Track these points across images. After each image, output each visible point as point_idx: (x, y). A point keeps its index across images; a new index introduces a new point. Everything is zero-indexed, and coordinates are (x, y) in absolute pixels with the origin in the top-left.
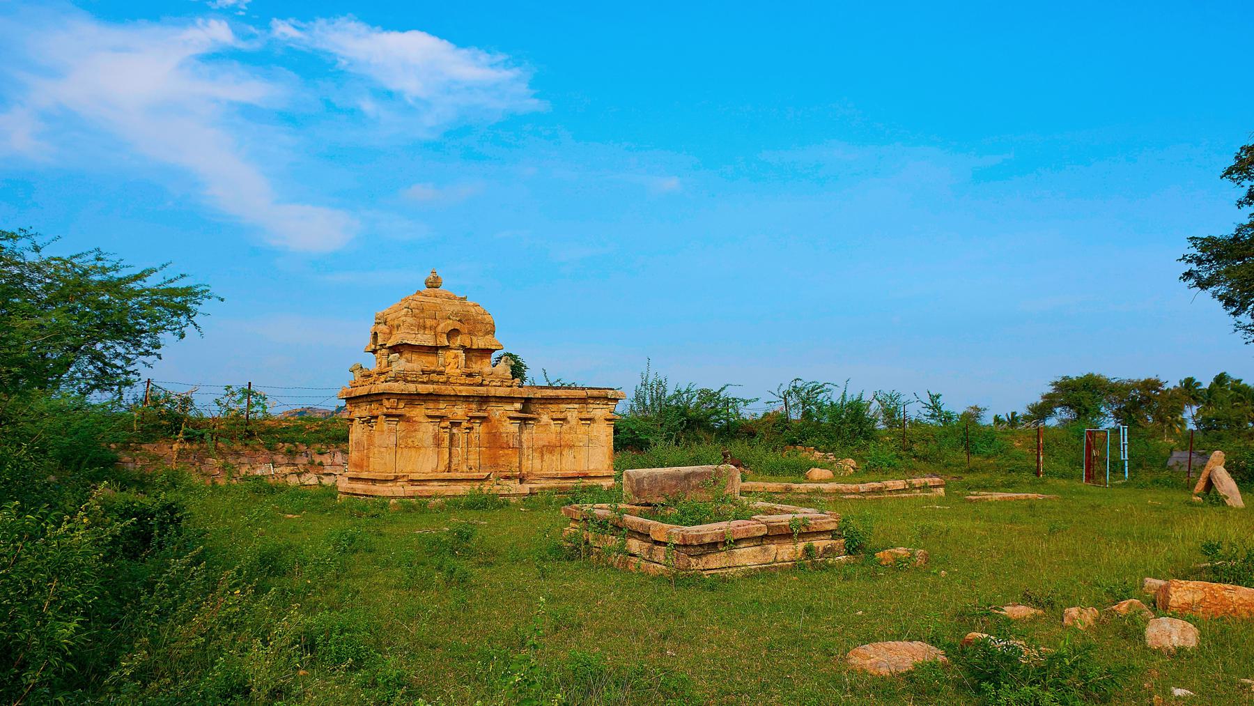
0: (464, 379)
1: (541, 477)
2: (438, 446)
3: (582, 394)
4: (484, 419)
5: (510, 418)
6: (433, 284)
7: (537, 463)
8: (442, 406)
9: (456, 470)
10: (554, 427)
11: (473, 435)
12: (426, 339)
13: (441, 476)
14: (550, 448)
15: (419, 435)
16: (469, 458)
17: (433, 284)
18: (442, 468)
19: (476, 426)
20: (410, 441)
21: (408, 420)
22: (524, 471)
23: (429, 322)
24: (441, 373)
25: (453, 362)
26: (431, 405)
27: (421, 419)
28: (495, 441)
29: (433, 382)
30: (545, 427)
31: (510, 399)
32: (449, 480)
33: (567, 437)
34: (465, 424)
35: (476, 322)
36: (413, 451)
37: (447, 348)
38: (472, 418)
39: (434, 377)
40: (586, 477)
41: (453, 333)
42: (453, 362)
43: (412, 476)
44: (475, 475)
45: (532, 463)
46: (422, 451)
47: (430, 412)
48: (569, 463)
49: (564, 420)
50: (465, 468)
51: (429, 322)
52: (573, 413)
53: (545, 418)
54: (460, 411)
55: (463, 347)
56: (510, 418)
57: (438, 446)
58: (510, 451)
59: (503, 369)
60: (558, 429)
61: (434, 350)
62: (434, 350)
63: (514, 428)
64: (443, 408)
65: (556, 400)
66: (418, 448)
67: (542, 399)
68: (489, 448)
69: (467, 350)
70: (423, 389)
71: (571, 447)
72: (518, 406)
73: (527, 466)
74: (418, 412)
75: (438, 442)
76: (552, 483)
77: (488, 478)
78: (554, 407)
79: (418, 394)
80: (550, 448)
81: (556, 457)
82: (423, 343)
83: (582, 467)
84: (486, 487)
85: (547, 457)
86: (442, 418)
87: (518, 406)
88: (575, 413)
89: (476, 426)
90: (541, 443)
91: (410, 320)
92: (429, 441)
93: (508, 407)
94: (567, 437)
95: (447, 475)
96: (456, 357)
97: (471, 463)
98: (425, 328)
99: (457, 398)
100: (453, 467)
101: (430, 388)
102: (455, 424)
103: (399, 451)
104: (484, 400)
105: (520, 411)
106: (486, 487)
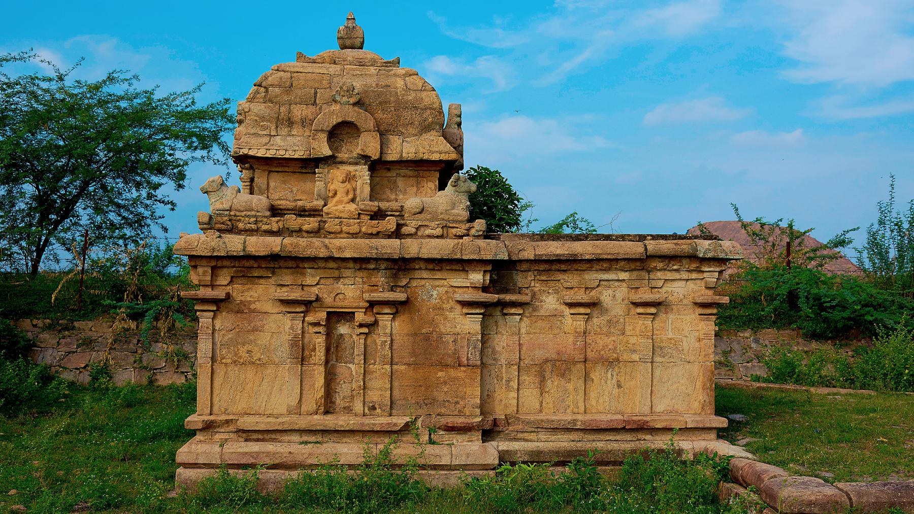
0: (368, 225)
1: (538, 427)
2: (303, 360)
3: (636, 249)
4: (399, 307)
5: (464, 304)
6: (350, 40)
7: (530, 397)
8: (309, 280)
9: (348, 410)
10: (572, 322)
11: (380, 338)
12: (291, 145)
13: (303, 422)
14: (561, 366)
15: (264, 339)
16: (372, 381)
17: (350, 40)
18: (310, 404)
19: (385, 321)
20: (242, 352)
21: (242, 310)
22: (500, 414)
23: (299, 112)
24: (314, 212)
25: (342, 191)
26: (288, 279)
27: (268, 307)
28: (427, 350)
29: (291, 232)
30: (551, 319)
31: (461, 265)
32: (324, 432)
33: (602, 341)
34: (360, 317)
35: (402, 105)
36: (250, 373)
37: (330, 161)
38: (372, 304)
39: (293, 221)
40: (642, 428)
41: (340, 132)
42: (342, 191)
43: (247, 422)
44: (381, 421)
45: (516, 397)
46: (270, 370)
47: (284, 294)
48: (605, 399)
49: (593, 305)
50: (358, 407)
51: (299, 112)
52: (615, 291)
53: (550, 302)
54: (350, 291)
55: (366, 158)
56: (464, 304)
57: (303, 360)
58: (461, 373)
59: (450, 201)
60: (580, 324)
61: (308, 165)
62: (308, 165)
63: (471, 324)
64: (313, 283)
65: (571, 263)
66: (260, 365)
67: (537, 261)
68: (415, 365)
69: (377, 166)
70: (258, 245)
71: (611, 363)
72: (477, 277)
73: (505, 402)
74: (262, 294)
75: (302, 356)
76: (563, 442)
77: (406, 428)
78: (569, 279)
79: (249, 257)
80: (561, 366)
81: (574, 384)
82: (281, 154)
83: (637, 406)
84: (403, 451)
85: (552, 384)
86: (308, 305)
87: (477, 277)
88: (622, 292)
89: (385, 321)
90: (540, 355)
91: (259, 108)
92: (282, 349)
93: (457, 280)
94: (602, 341)
95: (320, 421)
96: (349, 178)
97: (374, 396)
98: (290, 123)
99: (335, 264)
100: (339, 401)
101: (274, 244)
102: (336, 317)
103: (220, 371)
104: (401, 266)
105: (485, 289)
106: (403, 451)
